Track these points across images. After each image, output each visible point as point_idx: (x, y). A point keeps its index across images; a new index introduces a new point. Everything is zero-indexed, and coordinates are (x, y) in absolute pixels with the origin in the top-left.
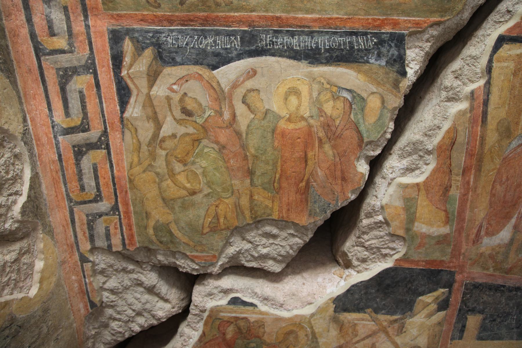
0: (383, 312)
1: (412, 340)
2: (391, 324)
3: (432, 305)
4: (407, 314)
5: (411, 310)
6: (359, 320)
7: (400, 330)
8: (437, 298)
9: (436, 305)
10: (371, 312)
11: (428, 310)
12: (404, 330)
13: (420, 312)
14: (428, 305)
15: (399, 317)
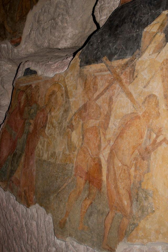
0: (116, 57)
1: (145, 87)
2: (123, 70)
3: (159, 34)
4: (135, 53)
5: (138, 47)
6: (98, 72)
7: (131, 76)
8: (162, 25)
9: (163, 34)
10: (106, 60)
11: (155, 42)
12: (135, 74)
13: (148, 46)
14: (154, 36)
15: (129, 58)
